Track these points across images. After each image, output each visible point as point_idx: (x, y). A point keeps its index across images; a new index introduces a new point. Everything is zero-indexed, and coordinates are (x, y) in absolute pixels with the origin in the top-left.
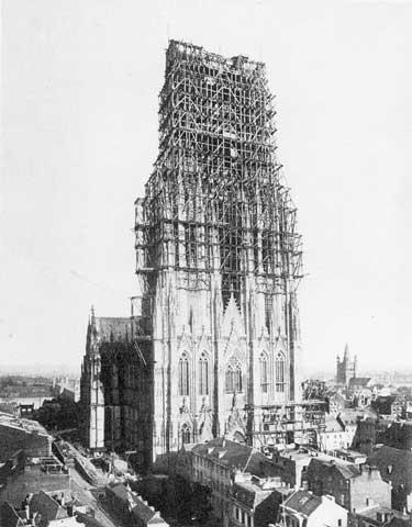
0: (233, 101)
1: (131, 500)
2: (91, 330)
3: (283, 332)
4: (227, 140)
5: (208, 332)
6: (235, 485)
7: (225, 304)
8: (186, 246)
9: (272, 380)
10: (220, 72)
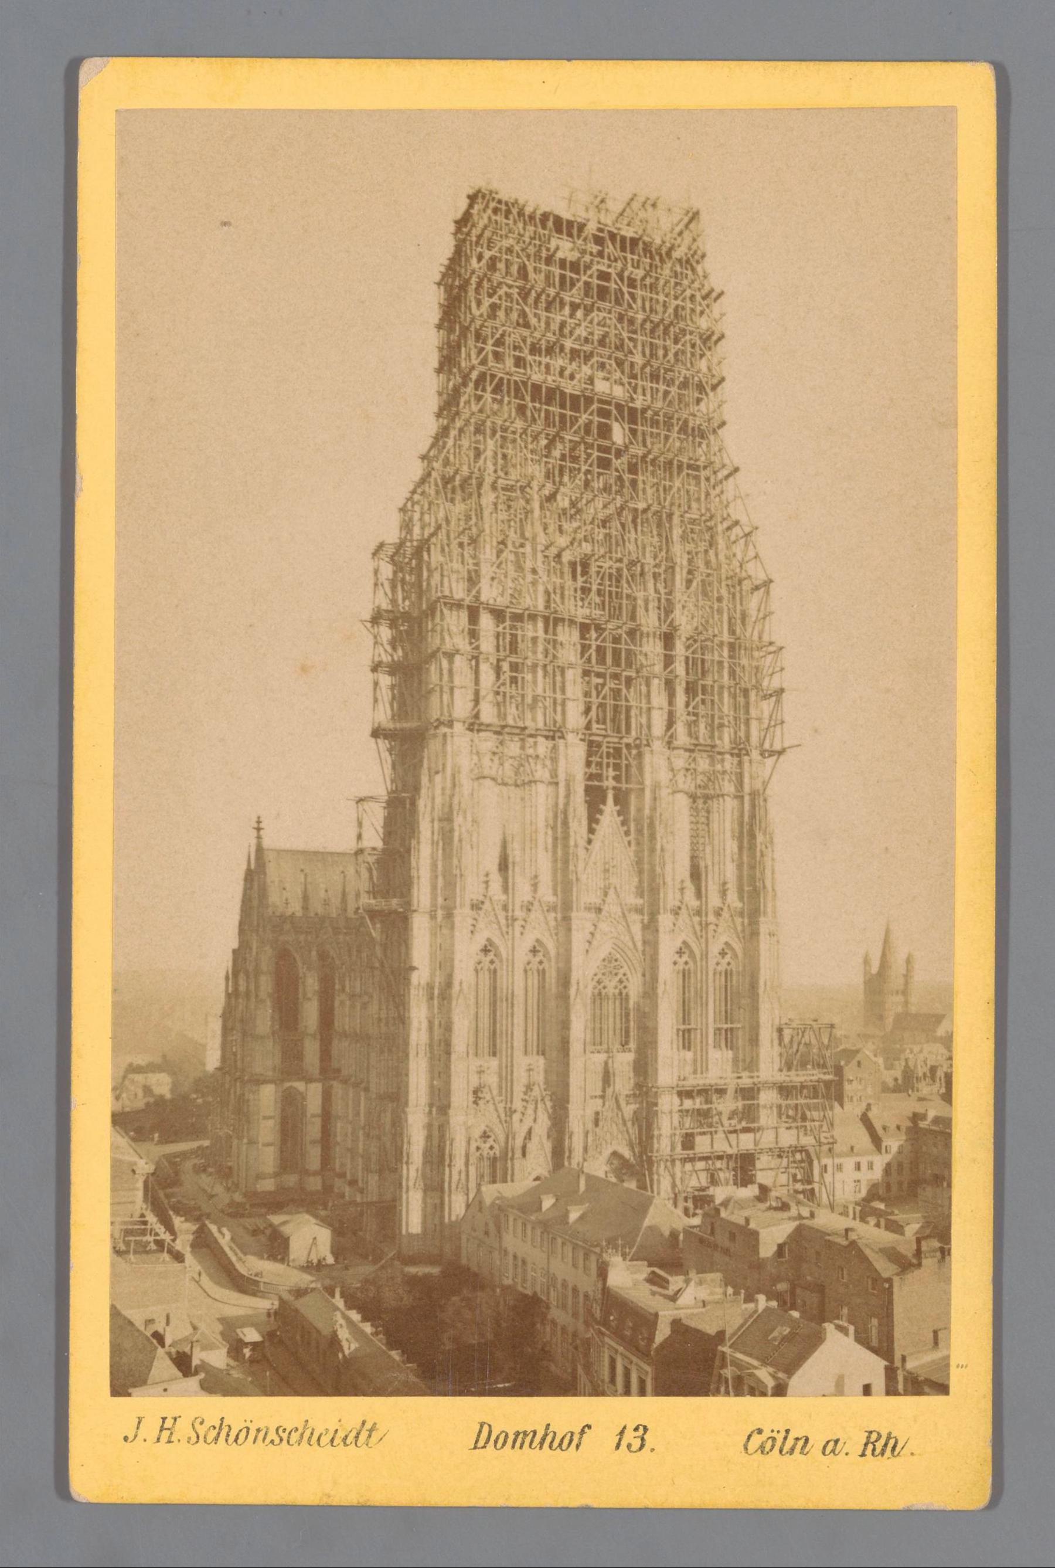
0: (618, 302)
1: (343, 1334)
2: (255, 877)
3: (732, 897)
4: (563, 457)
5: (546, 894)
6: (606, 1291)
7: (593, 820)
8: (498, 670)
9: (709, 1018)
10: (591, 228)
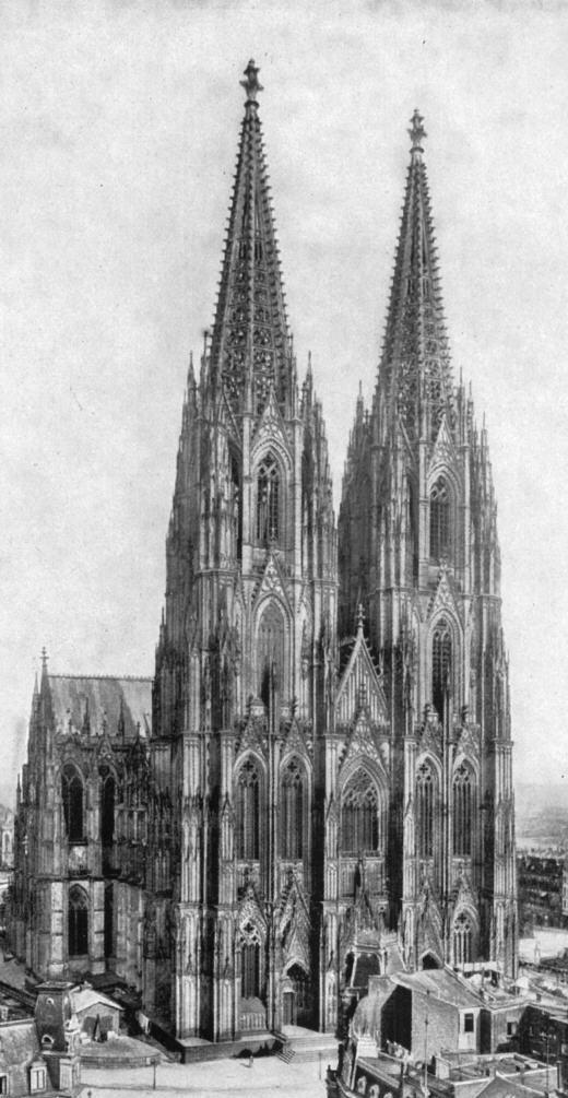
2: (44, 703)
